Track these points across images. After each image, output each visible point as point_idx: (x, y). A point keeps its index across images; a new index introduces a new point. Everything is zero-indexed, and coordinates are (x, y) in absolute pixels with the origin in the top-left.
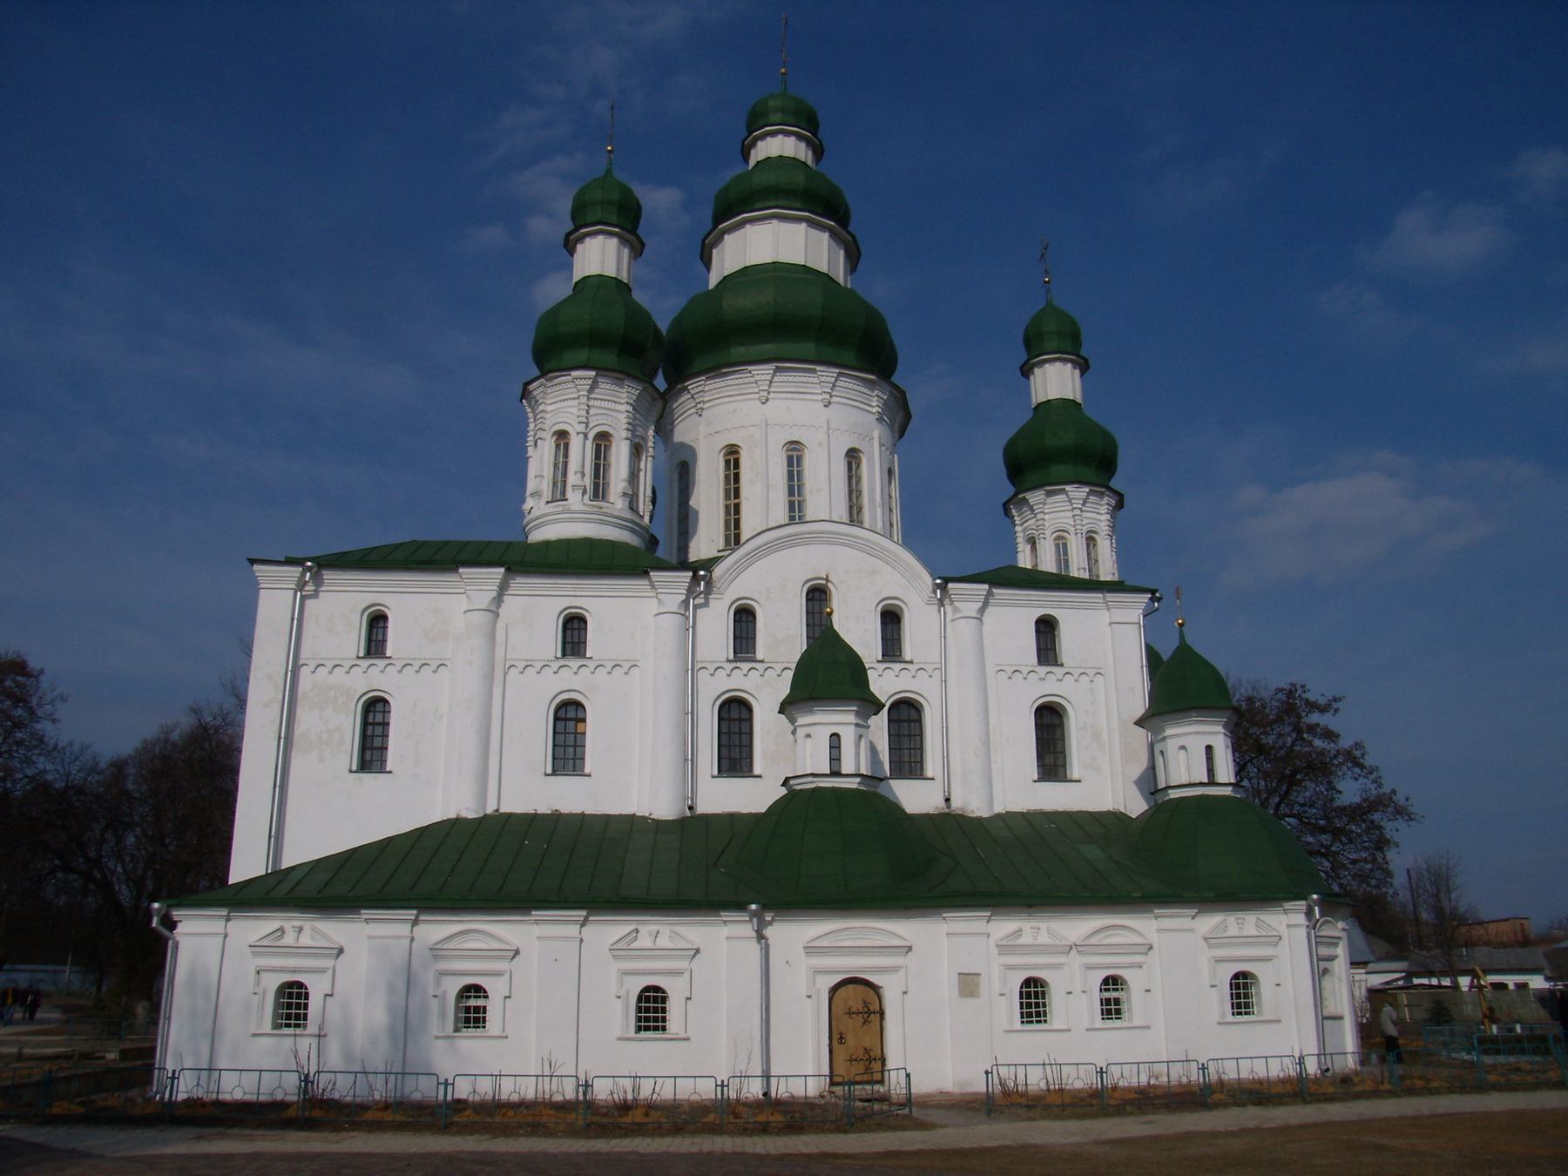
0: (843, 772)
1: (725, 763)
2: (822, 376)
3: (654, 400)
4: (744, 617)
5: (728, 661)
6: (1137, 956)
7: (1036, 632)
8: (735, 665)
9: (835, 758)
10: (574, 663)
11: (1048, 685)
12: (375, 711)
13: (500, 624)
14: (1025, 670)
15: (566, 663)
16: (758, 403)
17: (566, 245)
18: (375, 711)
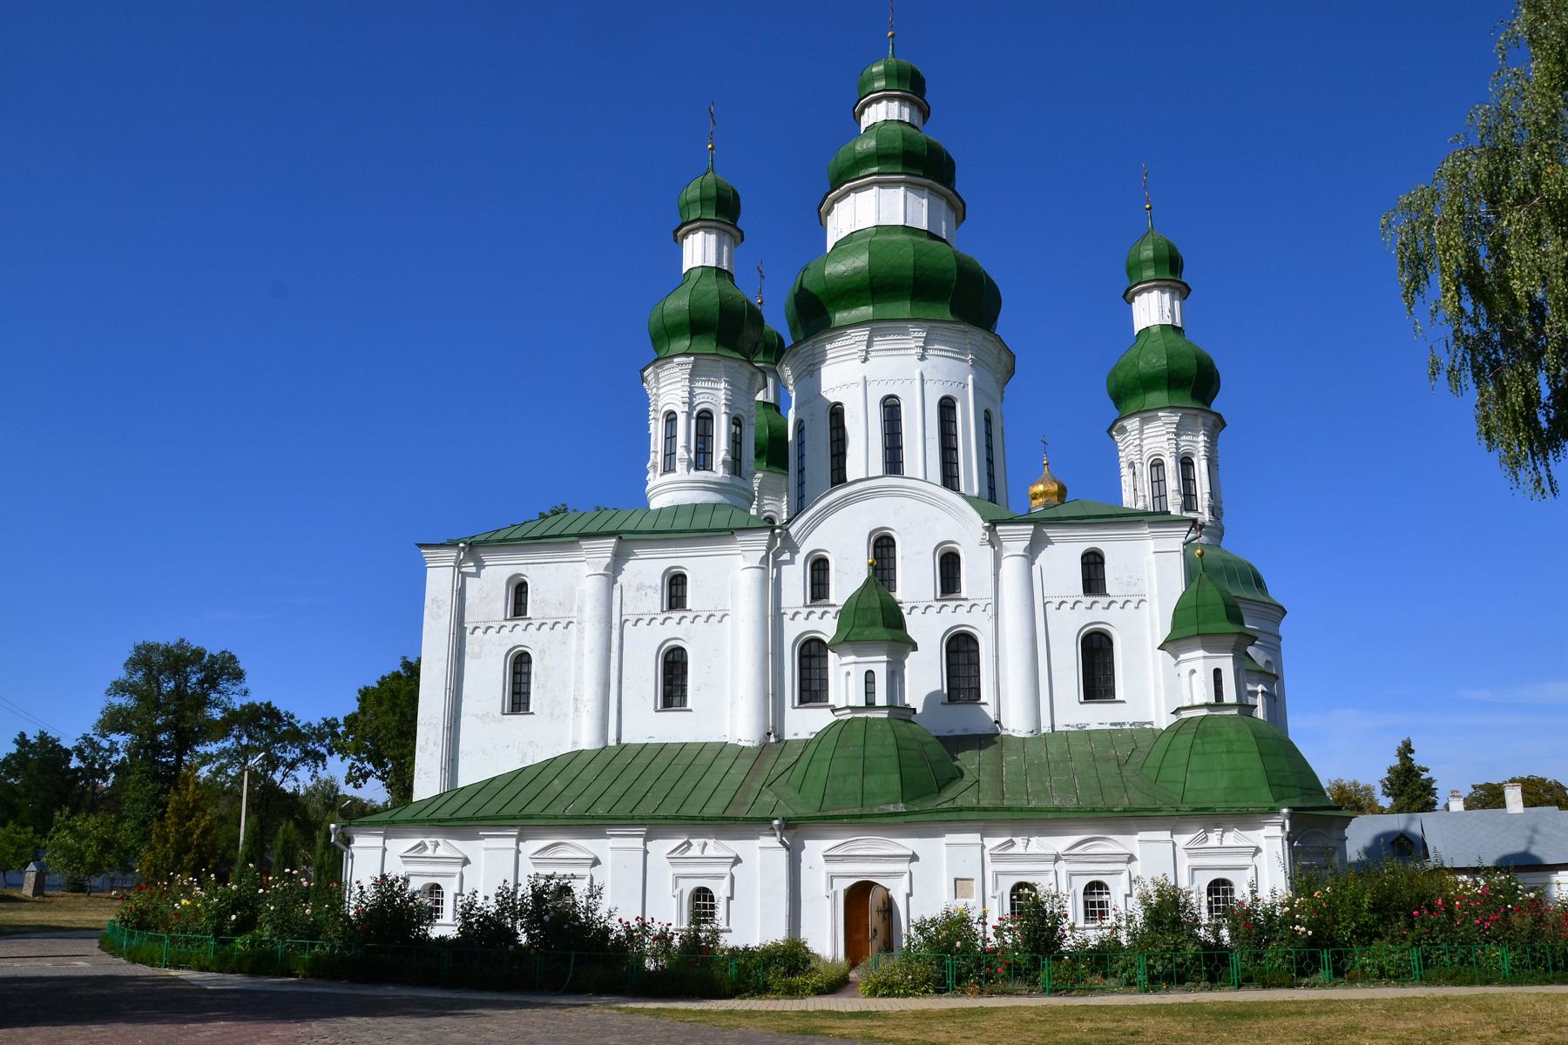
0: (877, 704)
1: (806, 695)
2: (914, 332)
5: (805, 606)
6: (1079, 865)
8: (810, 609)
9: (870, 692)
10: (676, 615)
12: (520, 664)
13: (617, 587)
14: (1071, 602)
15: (670, 615)
16: (858, 361)
18: (520, 664)
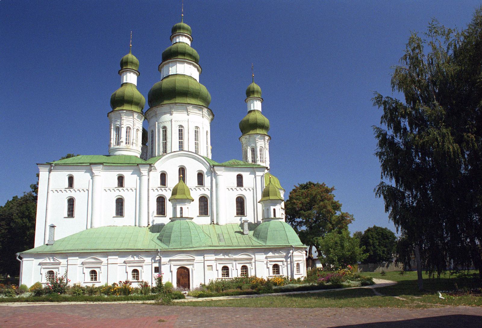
0: (183, 217)
3: (142, 117)
4: (163, 176)
7: (237, 178)
9: (181, 213)
10: (120, 189)
11: (240, 192)
12: (71, 202)
17: (119, 73)
18: (71, 202)
